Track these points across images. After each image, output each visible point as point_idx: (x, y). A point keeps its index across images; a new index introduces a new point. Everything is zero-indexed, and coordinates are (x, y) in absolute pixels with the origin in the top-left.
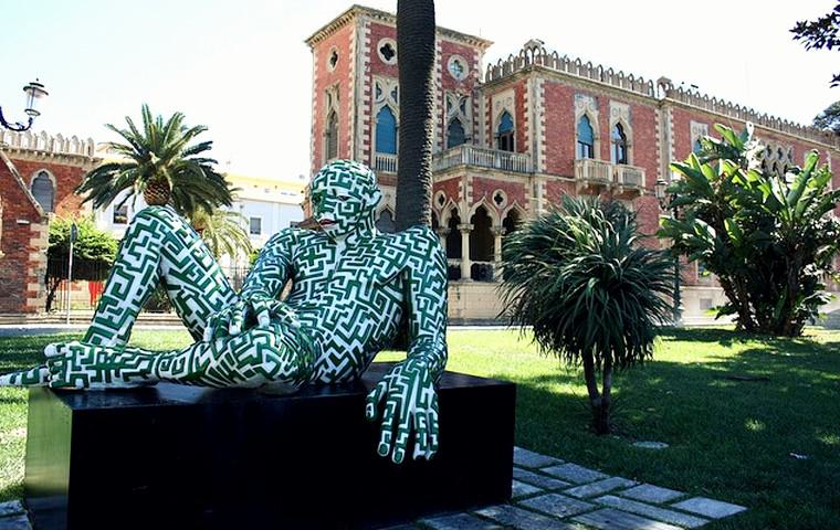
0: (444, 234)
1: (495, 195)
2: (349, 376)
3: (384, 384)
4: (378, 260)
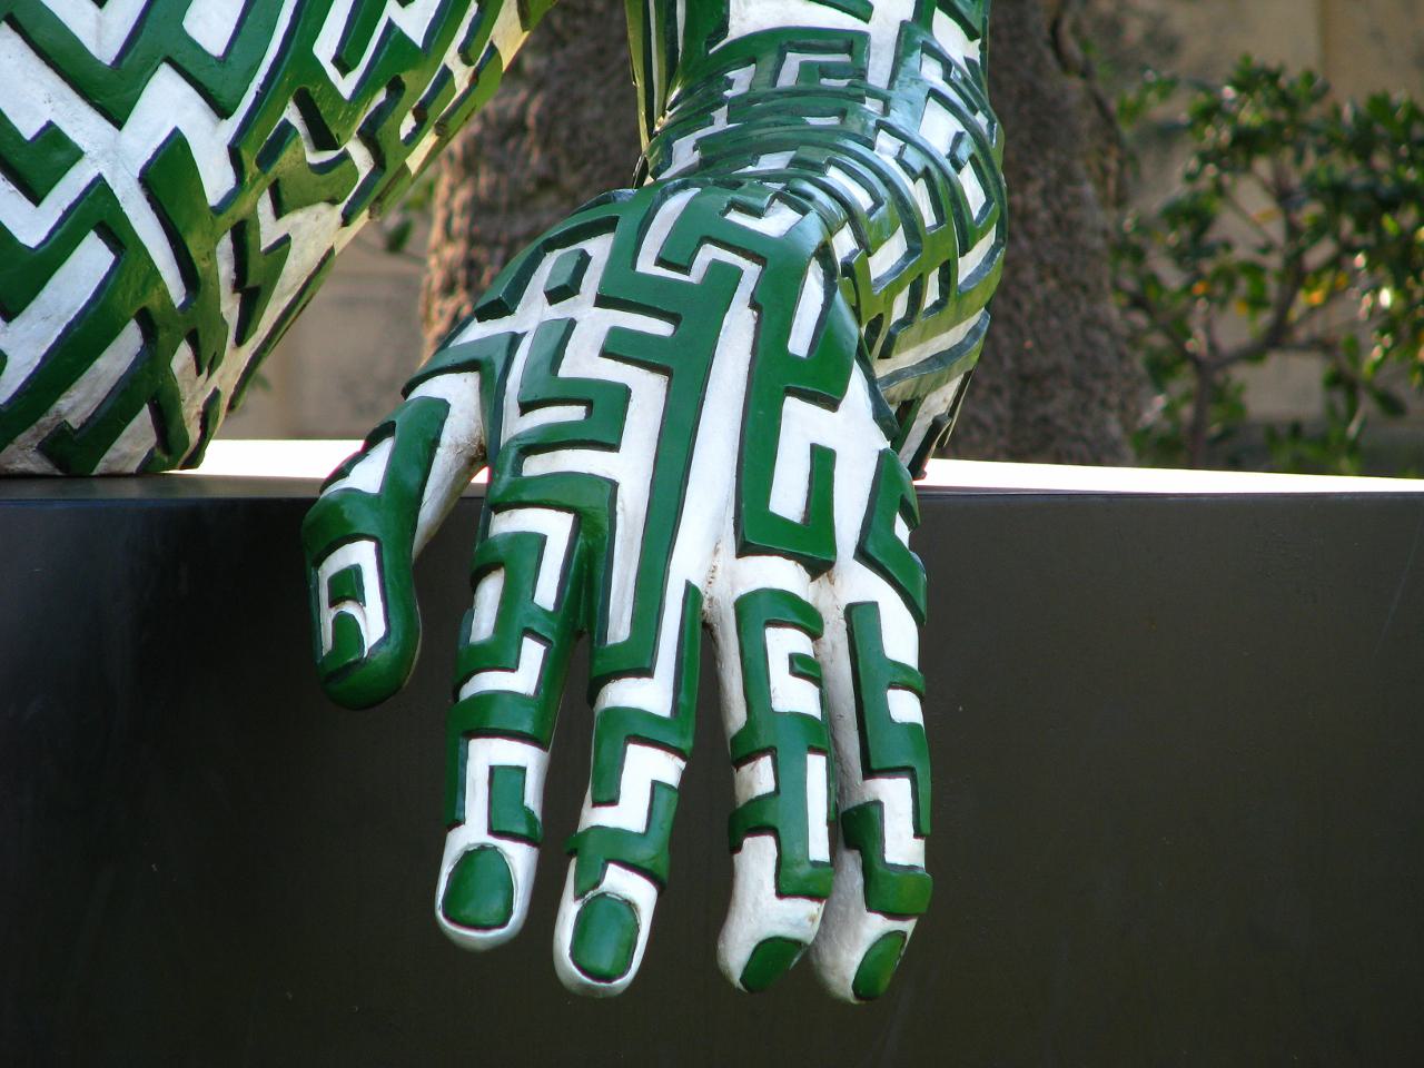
2: (109, 421)
3: (458, 392)
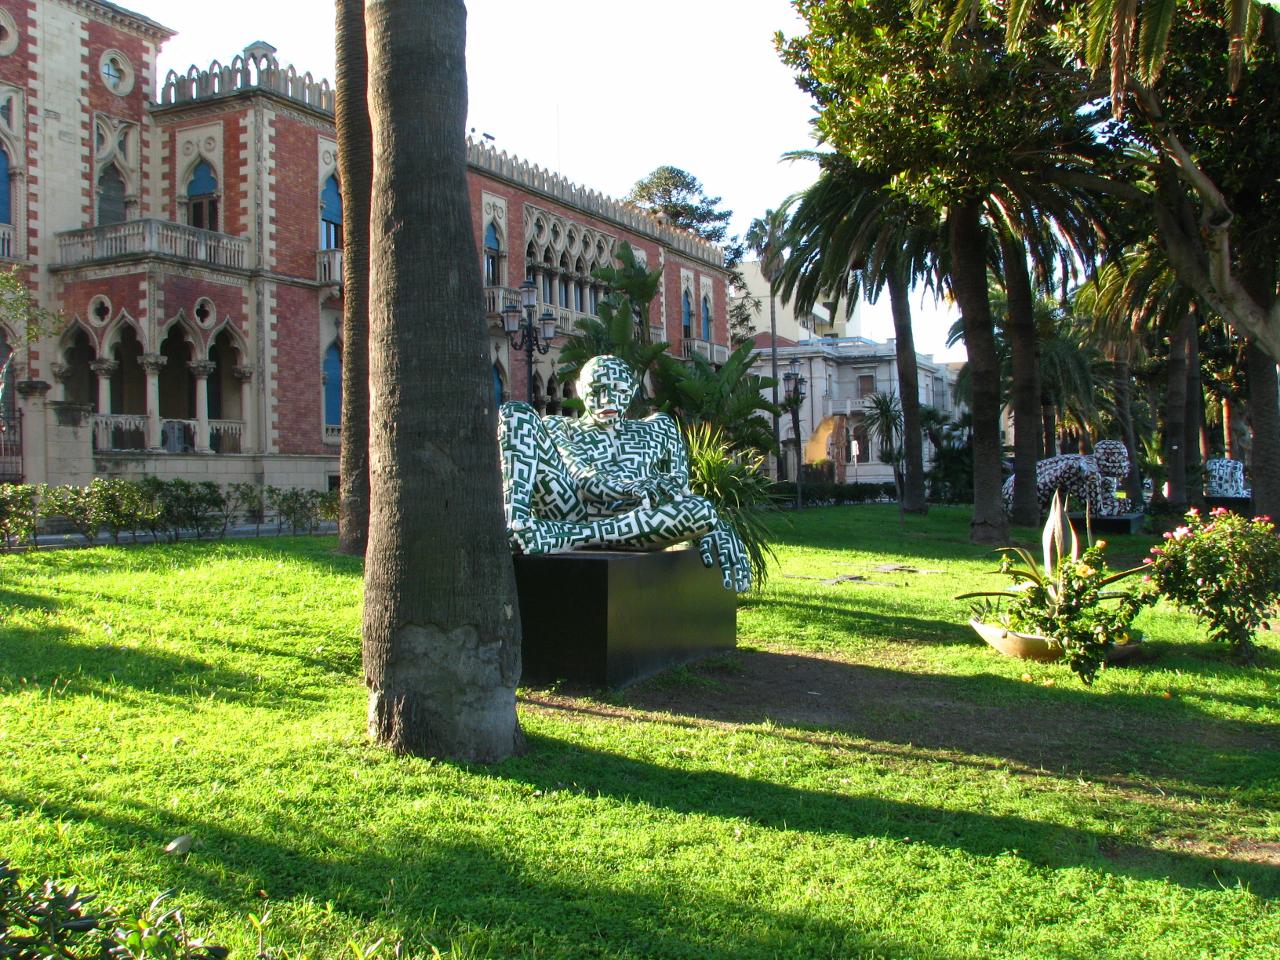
0: (108, 371)
1: (197, 307)
4: (652, 444)
